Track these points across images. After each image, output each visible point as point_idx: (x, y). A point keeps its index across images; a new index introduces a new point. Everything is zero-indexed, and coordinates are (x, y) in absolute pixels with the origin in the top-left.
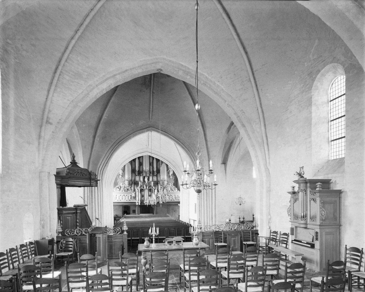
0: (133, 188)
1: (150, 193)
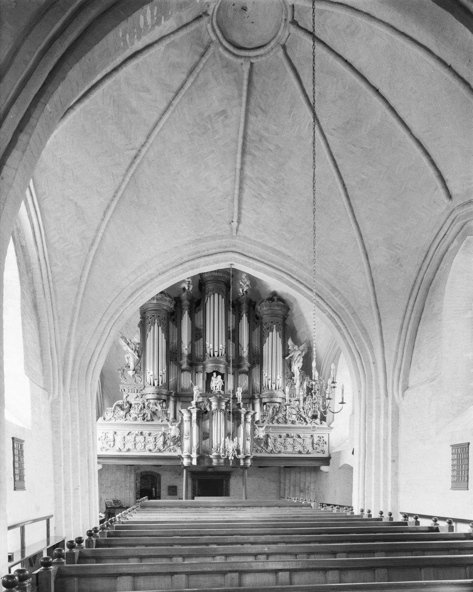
0: (171, 411)
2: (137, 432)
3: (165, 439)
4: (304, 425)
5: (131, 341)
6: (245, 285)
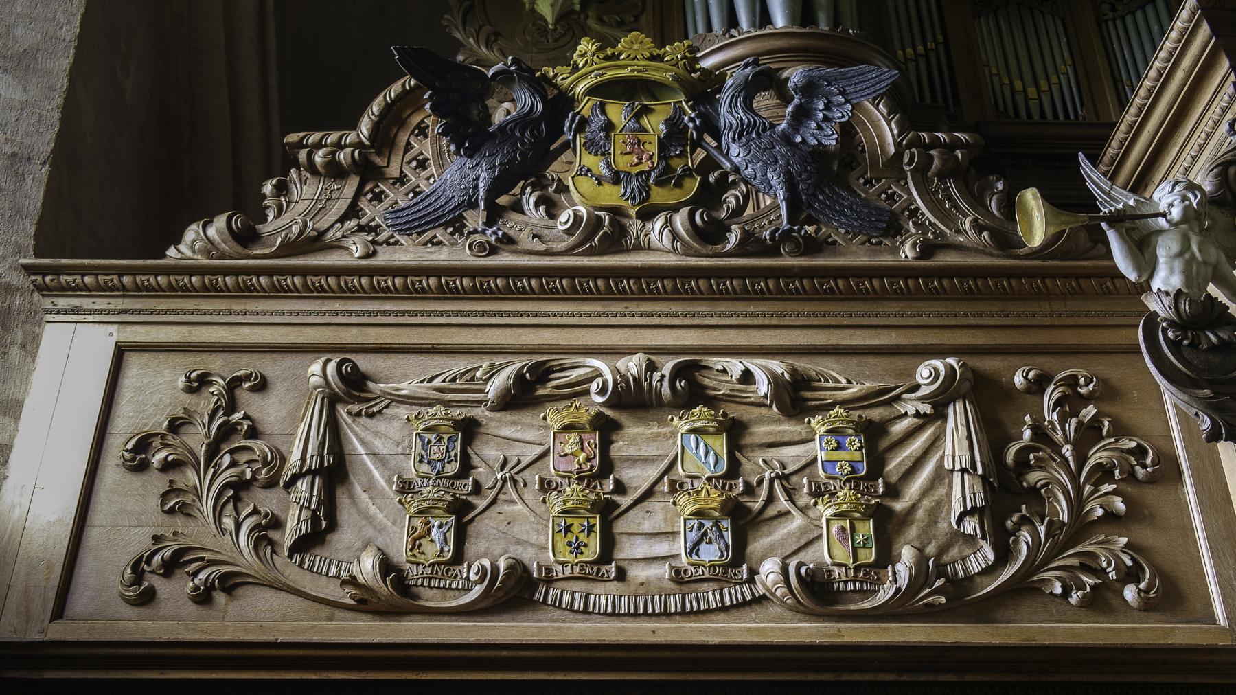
2: (633, 365)
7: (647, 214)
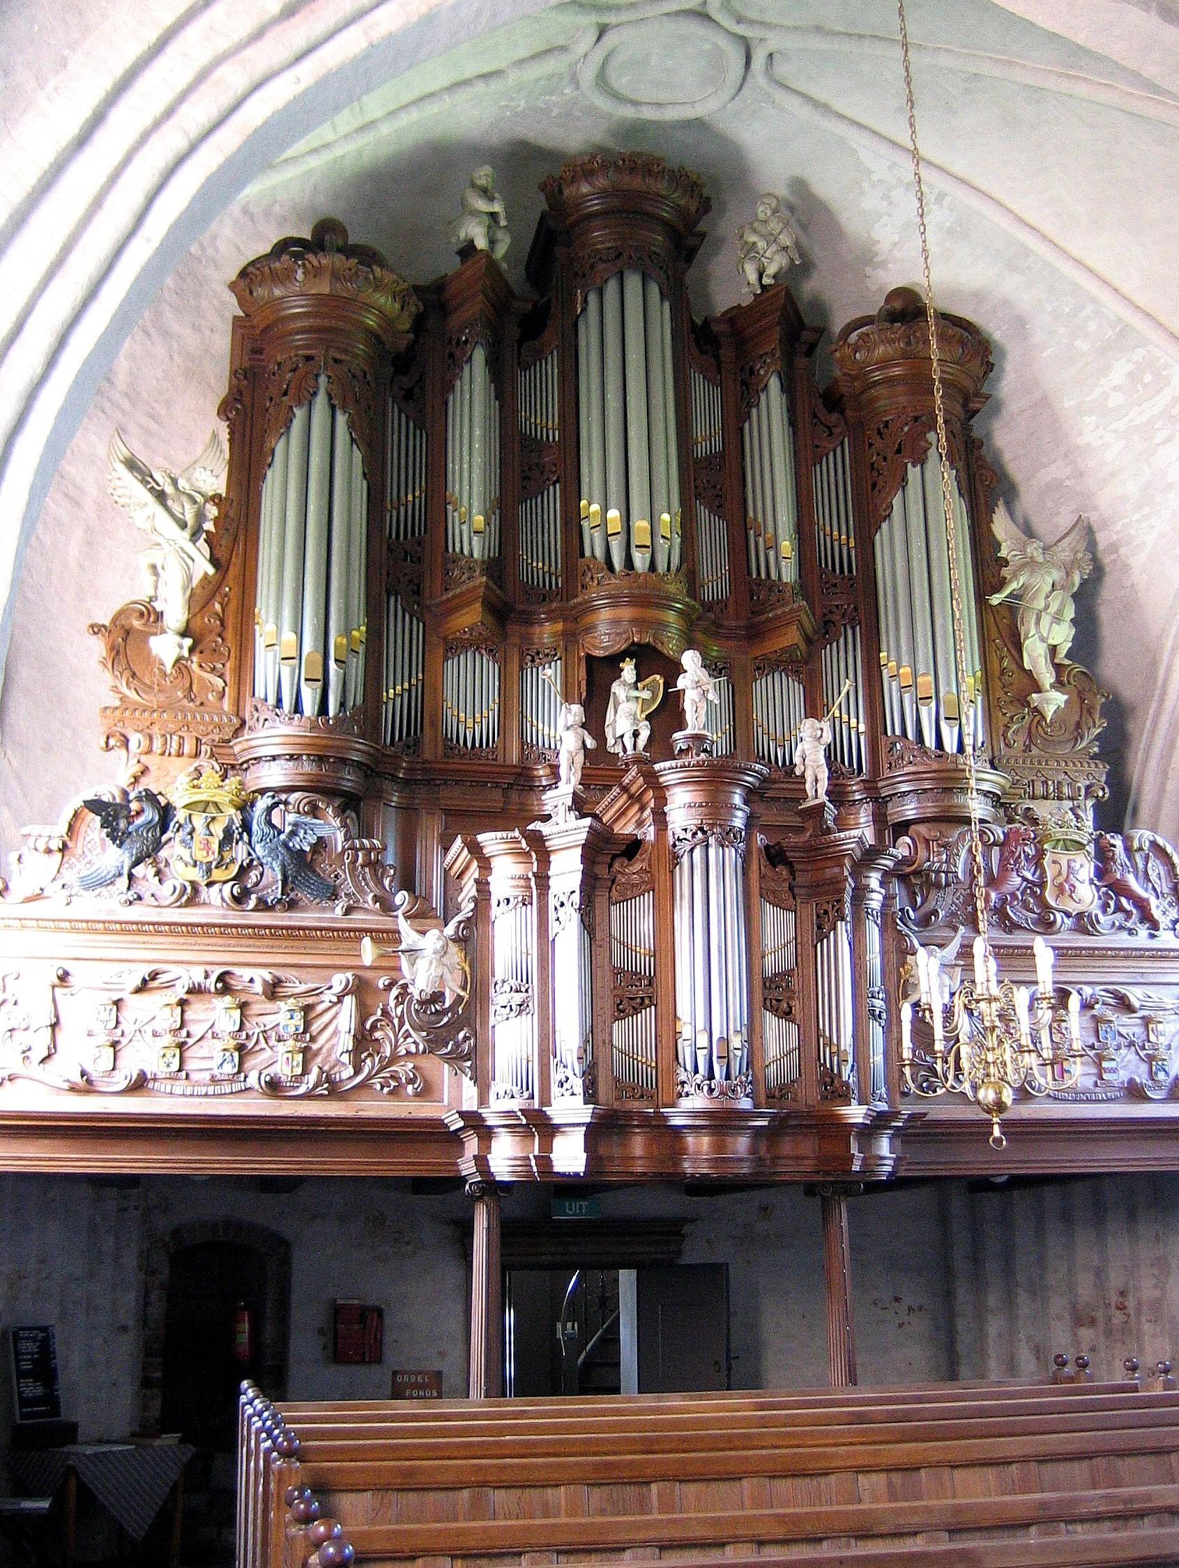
1: (777, 926)
2: (197, 975)
3: (362, 1020)
4: (1142, 938)
5: (174, 482)
6: (774, 248)
7: (210, 885)
